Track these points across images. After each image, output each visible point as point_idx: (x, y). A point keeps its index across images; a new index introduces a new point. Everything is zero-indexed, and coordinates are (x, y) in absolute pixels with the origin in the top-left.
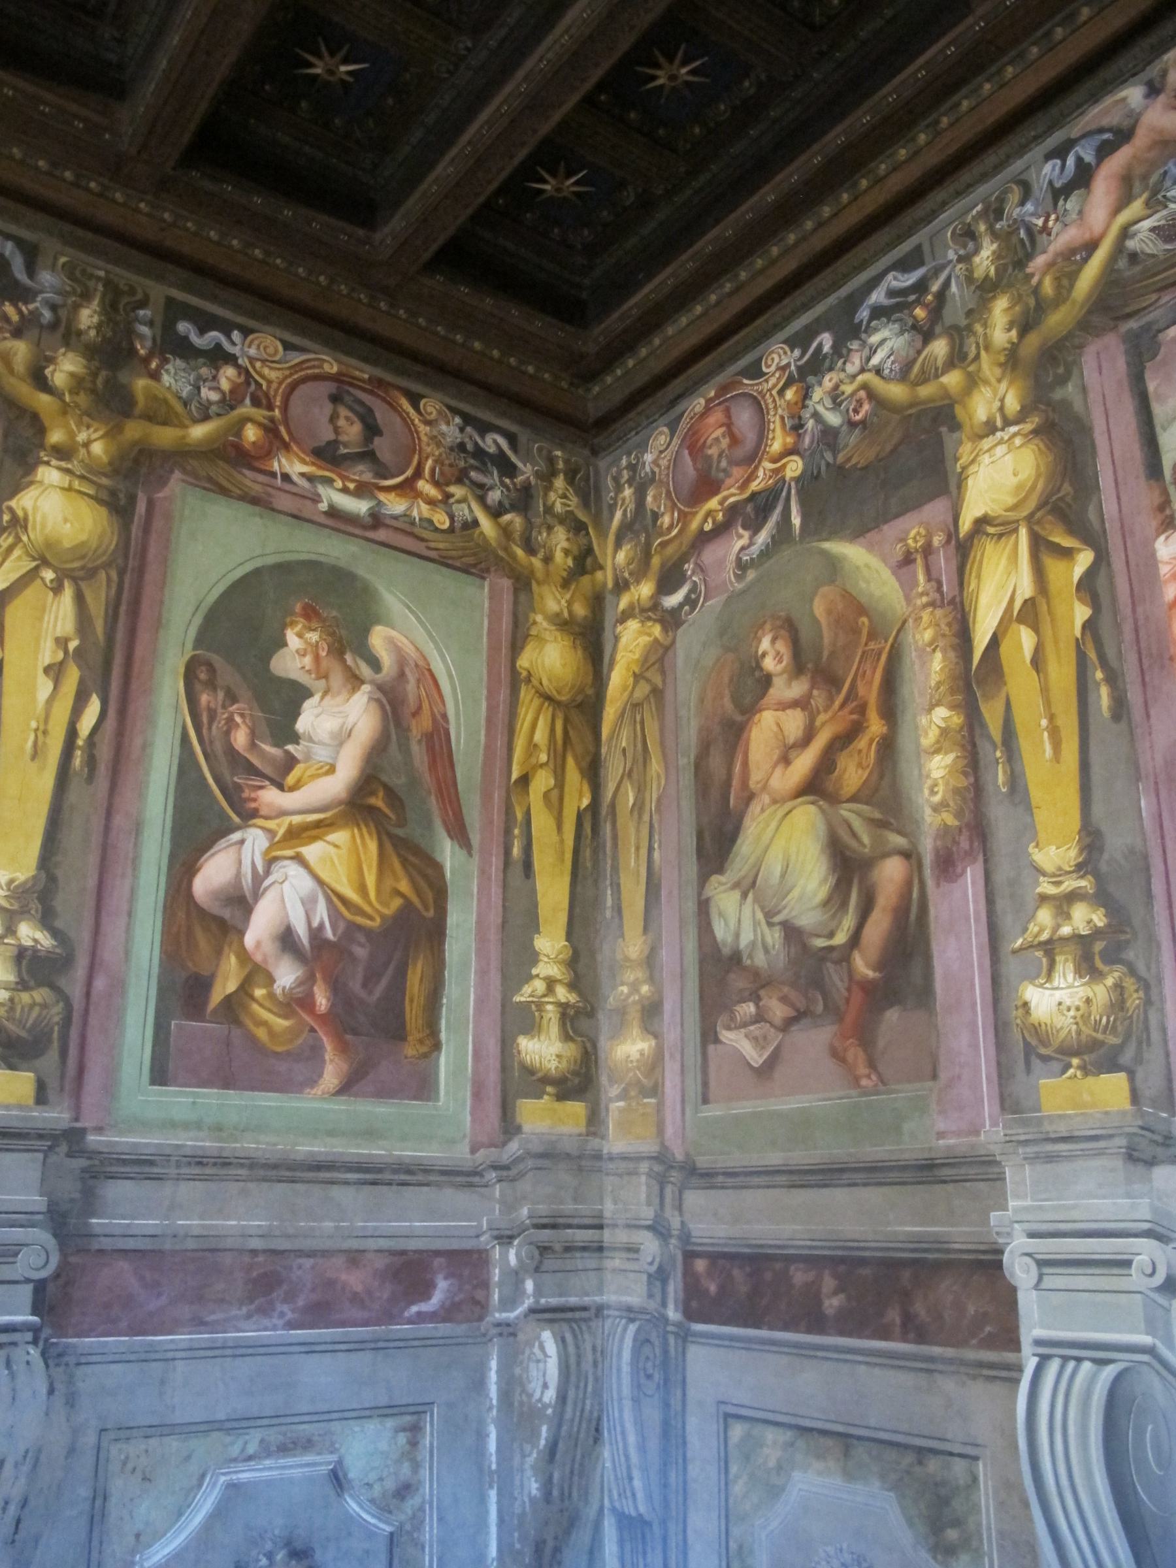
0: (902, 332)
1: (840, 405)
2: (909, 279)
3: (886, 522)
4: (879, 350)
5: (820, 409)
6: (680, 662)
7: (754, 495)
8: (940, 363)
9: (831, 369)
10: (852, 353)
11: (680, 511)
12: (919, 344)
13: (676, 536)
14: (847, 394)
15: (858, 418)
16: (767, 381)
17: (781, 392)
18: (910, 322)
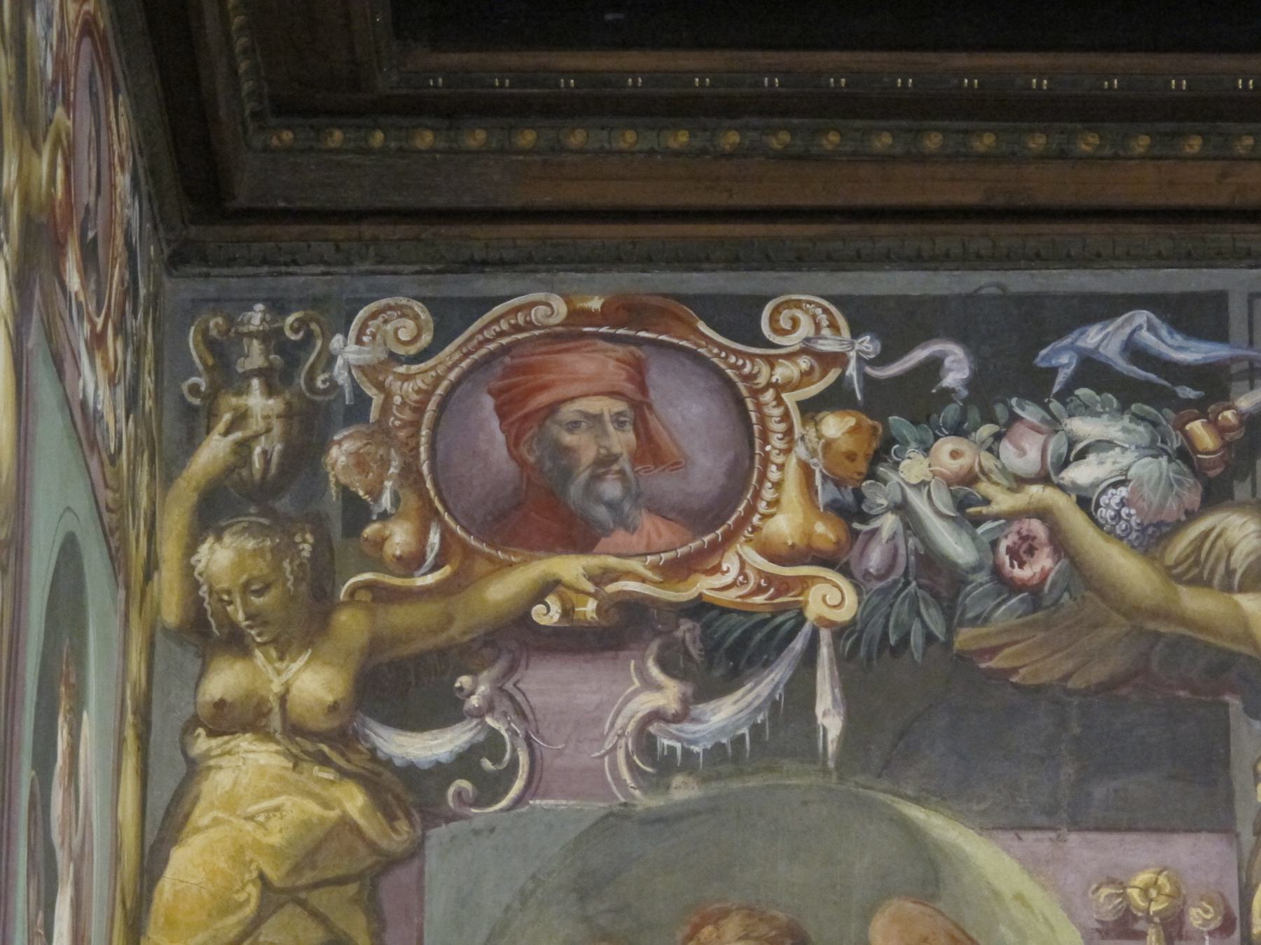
0: (1154, 449)
1: (977, 521)
2: (1193, 353)
3: (1077, 825)
4: (1092, 457)
5: (918, 502)
6: (438, 905)
7: (699, 608)
8: (1240, 561)
9: (958, 430)
10: (1018, 428)
11: (446, 534)
12: (1193, 497)
13: (427, 592)
14: (994, 508)
15: (1023, 573)
16: (771, 362)
17: (811, 409)
18: (1176, 442)
